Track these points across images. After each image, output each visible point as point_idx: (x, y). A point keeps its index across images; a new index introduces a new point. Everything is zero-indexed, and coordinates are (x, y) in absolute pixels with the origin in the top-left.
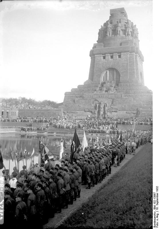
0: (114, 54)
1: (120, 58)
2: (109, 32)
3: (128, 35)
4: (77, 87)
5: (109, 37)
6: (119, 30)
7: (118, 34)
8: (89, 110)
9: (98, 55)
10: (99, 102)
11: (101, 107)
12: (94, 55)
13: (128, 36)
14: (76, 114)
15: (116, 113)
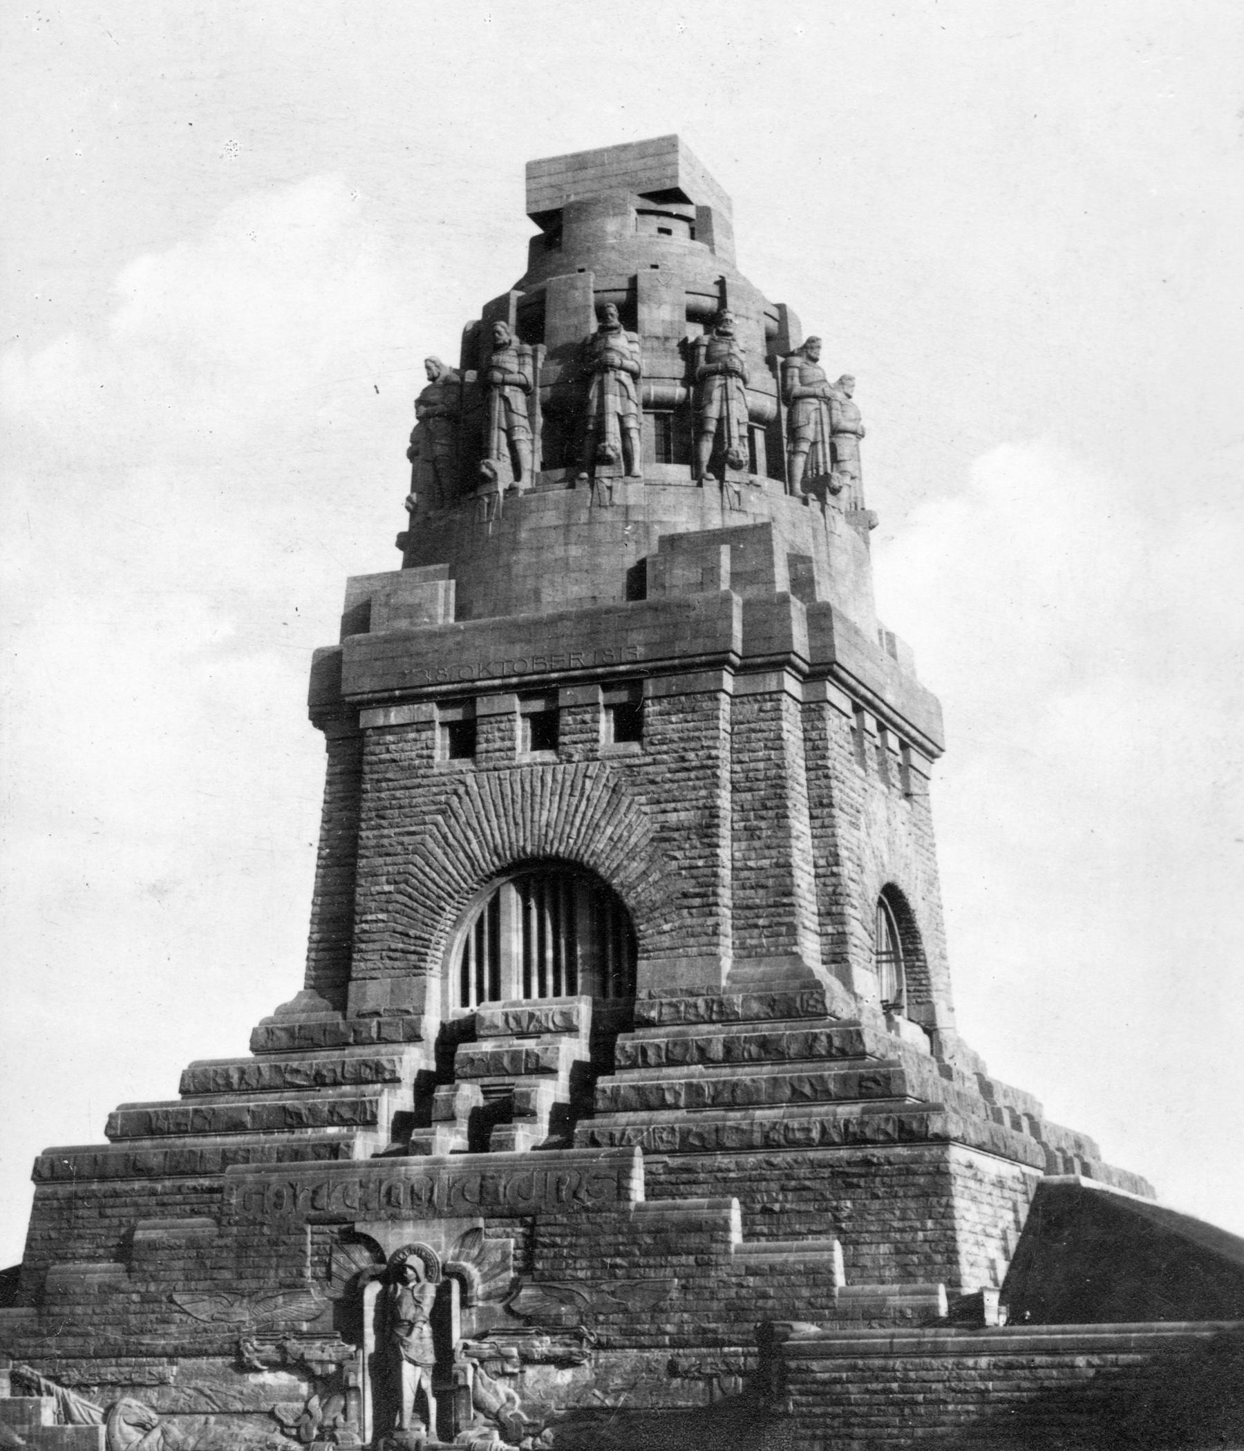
0: (567, 696)
1: (635, 747)
2: (509, 432)
3: (720, 463)
4: (168, 1091)
5: (511, 490)
6: (614, 403)
7: (608, 461)
8: (282, 1349)
9: (396, 716)
10: (388, 1255)
11: (408, 1310)
12: (355, 718)
13: (720, 477)
14: (153, 1394)
15: (564, 1377)
